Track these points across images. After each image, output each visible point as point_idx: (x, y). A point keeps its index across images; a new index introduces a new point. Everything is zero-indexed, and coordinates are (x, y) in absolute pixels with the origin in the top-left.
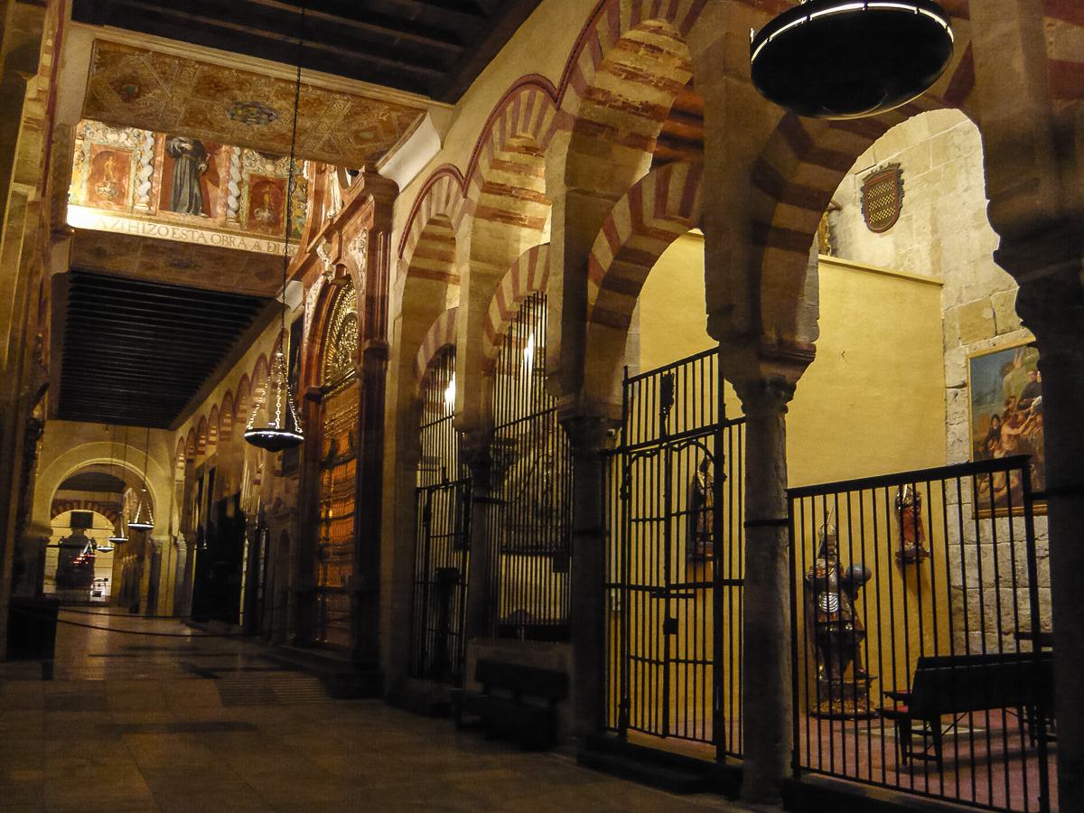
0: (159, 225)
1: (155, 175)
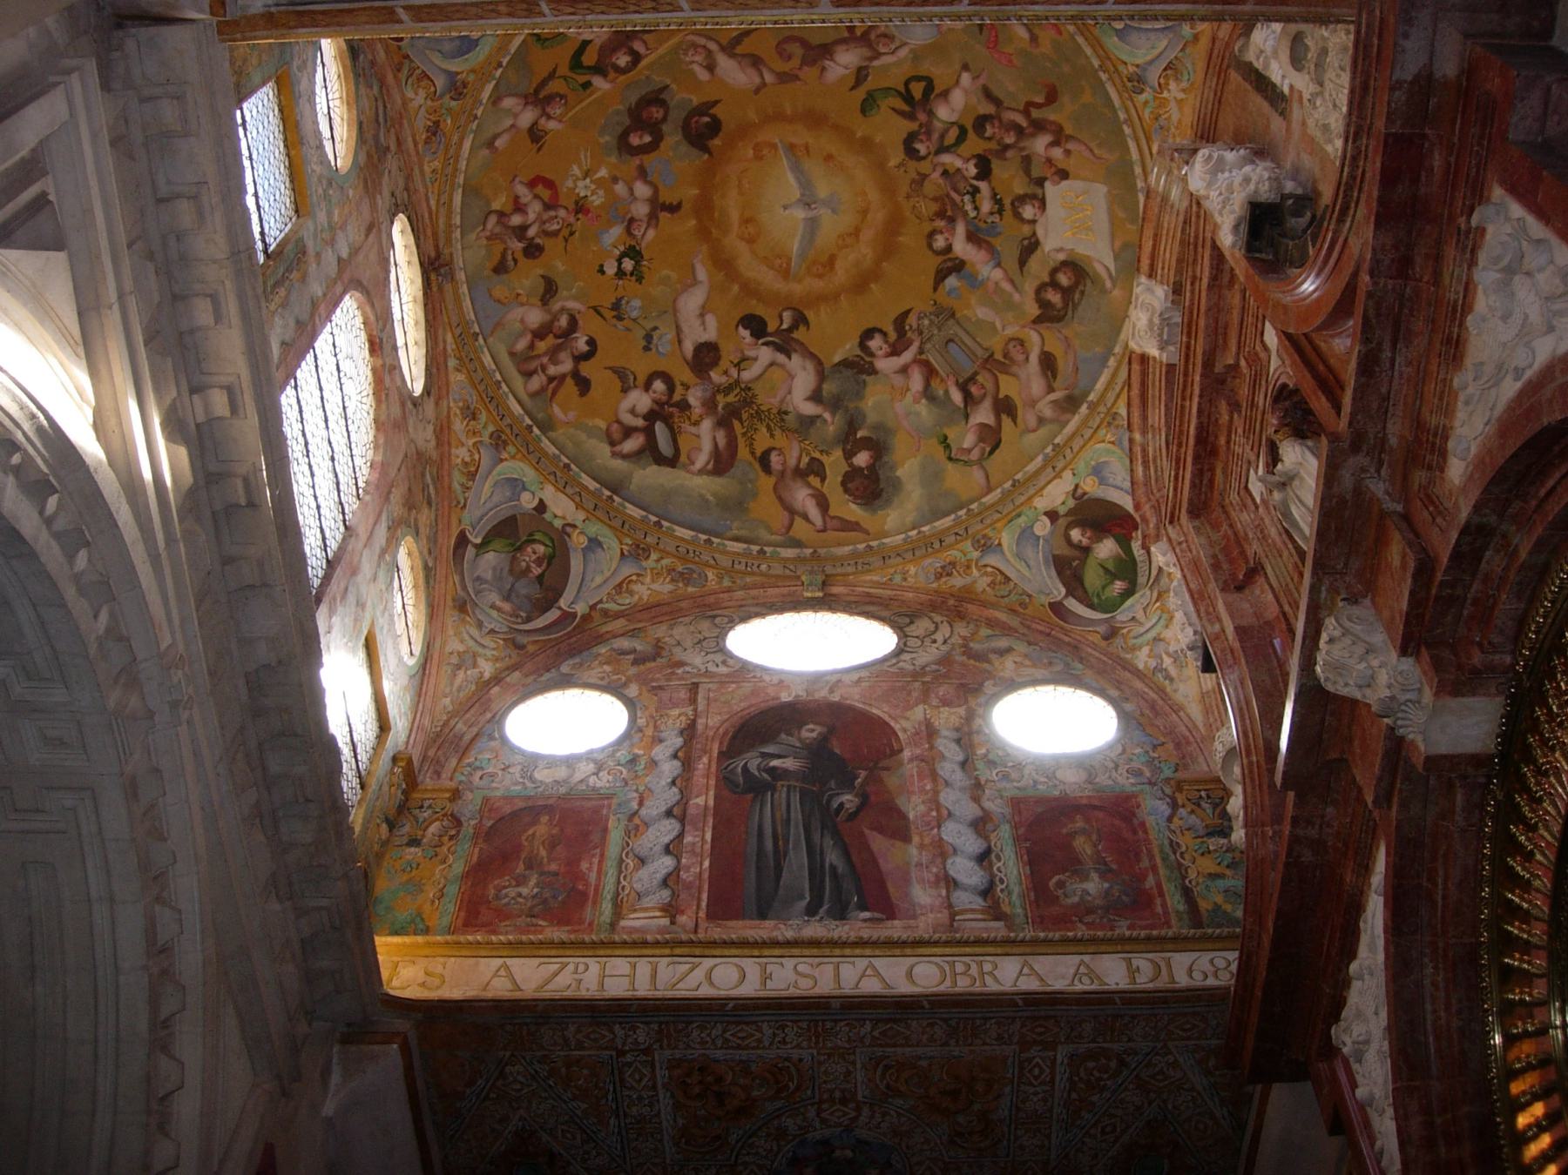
0: (708, 963)
1: (688, 839)
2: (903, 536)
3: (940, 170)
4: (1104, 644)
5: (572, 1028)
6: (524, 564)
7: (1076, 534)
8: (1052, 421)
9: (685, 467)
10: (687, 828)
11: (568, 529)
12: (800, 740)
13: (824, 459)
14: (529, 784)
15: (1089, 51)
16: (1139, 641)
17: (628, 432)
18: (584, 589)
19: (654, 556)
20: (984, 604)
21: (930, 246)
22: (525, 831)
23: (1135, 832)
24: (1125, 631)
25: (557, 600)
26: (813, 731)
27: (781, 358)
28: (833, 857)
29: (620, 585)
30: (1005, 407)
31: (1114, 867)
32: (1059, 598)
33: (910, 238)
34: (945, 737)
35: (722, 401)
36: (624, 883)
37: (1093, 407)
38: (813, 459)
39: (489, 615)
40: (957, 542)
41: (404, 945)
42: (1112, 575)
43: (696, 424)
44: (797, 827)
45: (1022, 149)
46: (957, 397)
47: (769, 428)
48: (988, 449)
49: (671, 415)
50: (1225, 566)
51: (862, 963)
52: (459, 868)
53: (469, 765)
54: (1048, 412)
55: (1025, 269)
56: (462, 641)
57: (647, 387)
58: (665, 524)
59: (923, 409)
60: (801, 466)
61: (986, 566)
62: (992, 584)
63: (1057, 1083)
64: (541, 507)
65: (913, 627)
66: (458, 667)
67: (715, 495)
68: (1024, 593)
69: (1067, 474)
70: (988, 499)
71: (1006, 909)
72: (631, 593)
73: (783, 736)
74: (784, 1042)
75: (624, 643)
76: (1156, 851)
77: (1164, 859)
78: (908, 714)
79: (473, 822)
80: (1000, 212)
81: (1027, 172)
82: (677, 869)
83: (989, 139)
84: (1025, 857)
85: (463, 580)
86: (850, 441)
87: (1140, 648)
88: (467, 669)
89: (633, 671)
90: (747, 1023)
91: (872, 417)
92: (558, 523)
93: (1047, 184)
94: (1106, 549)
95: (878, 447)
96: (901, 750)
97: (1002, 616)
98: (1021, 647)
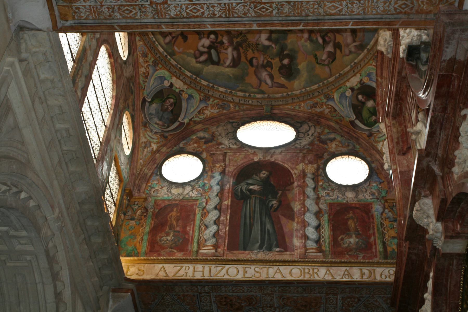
0: (227, 267)
1: (222, 218)
2: (300, 91)
4: (367, 138)
5: (185, 287)
6: (166, 107)
7: (360, 97)
8: (355, 53)
9: (222, 65)
10: (222, 214)
11: (181, 92)
12: (260, 178)
13: (273, 61)
14: (170, 195)
16: (380, 139)
17: (202, 53)
18: (187, 114)
19: (211, 100)
20: (327, 119)
22: (169, 214)
23: (369, 219)
24: (375, 135)
25: (178, 118)
26: (264, 174)
28: (268, 226)
29: (200, 111)
30: (337, 46)
31: (361, 233)
32: (353, 119)
34: (309, 177)
35: (235, 41)
36: (201, 236)
37: (368, 50)
38: (268, 61)
39: (155, 127)
40: (318, 96)
41: (131, 260)
43: (226, 49)
44: (257, 213)
46: (320, 41)
47: (252, 50)
48: (331, 61)
49: (217, 47)
50: (401, 143)
51: (276, 268)
52: (147, 229)
53: (150, 186)
54: (353, 49)
56: (146, 138)
57: (208, 37)
58: (215, 86)
59: (308, 44)
60: (264, 64)
61: (328, 105)
62: (330, 112)
63: (338, 305)
64: (172, 85)
65: (301, 128)
66: (145, 147)
68: (341, 116)
69: (358, 75)
70: (331, 80)
71: (323, 248)
72: (204, 114)
73: (254, 176)
74: (251, 291)
75: (201, 134)
76: (375, 227)
77: (378, 230)
78: (297, 167)
79: (152, 210)
82: (218, 230)
84: (332, 228)
85: (145, 116)
86: (281, 55)
88: (148, 148)
89: (204, 147)
90: (239, 286)
91: (289, 47)
92: (177, 90)
95: (292, 57)
96: (294, 183)
97: (333, 124)
98: (339, 138)
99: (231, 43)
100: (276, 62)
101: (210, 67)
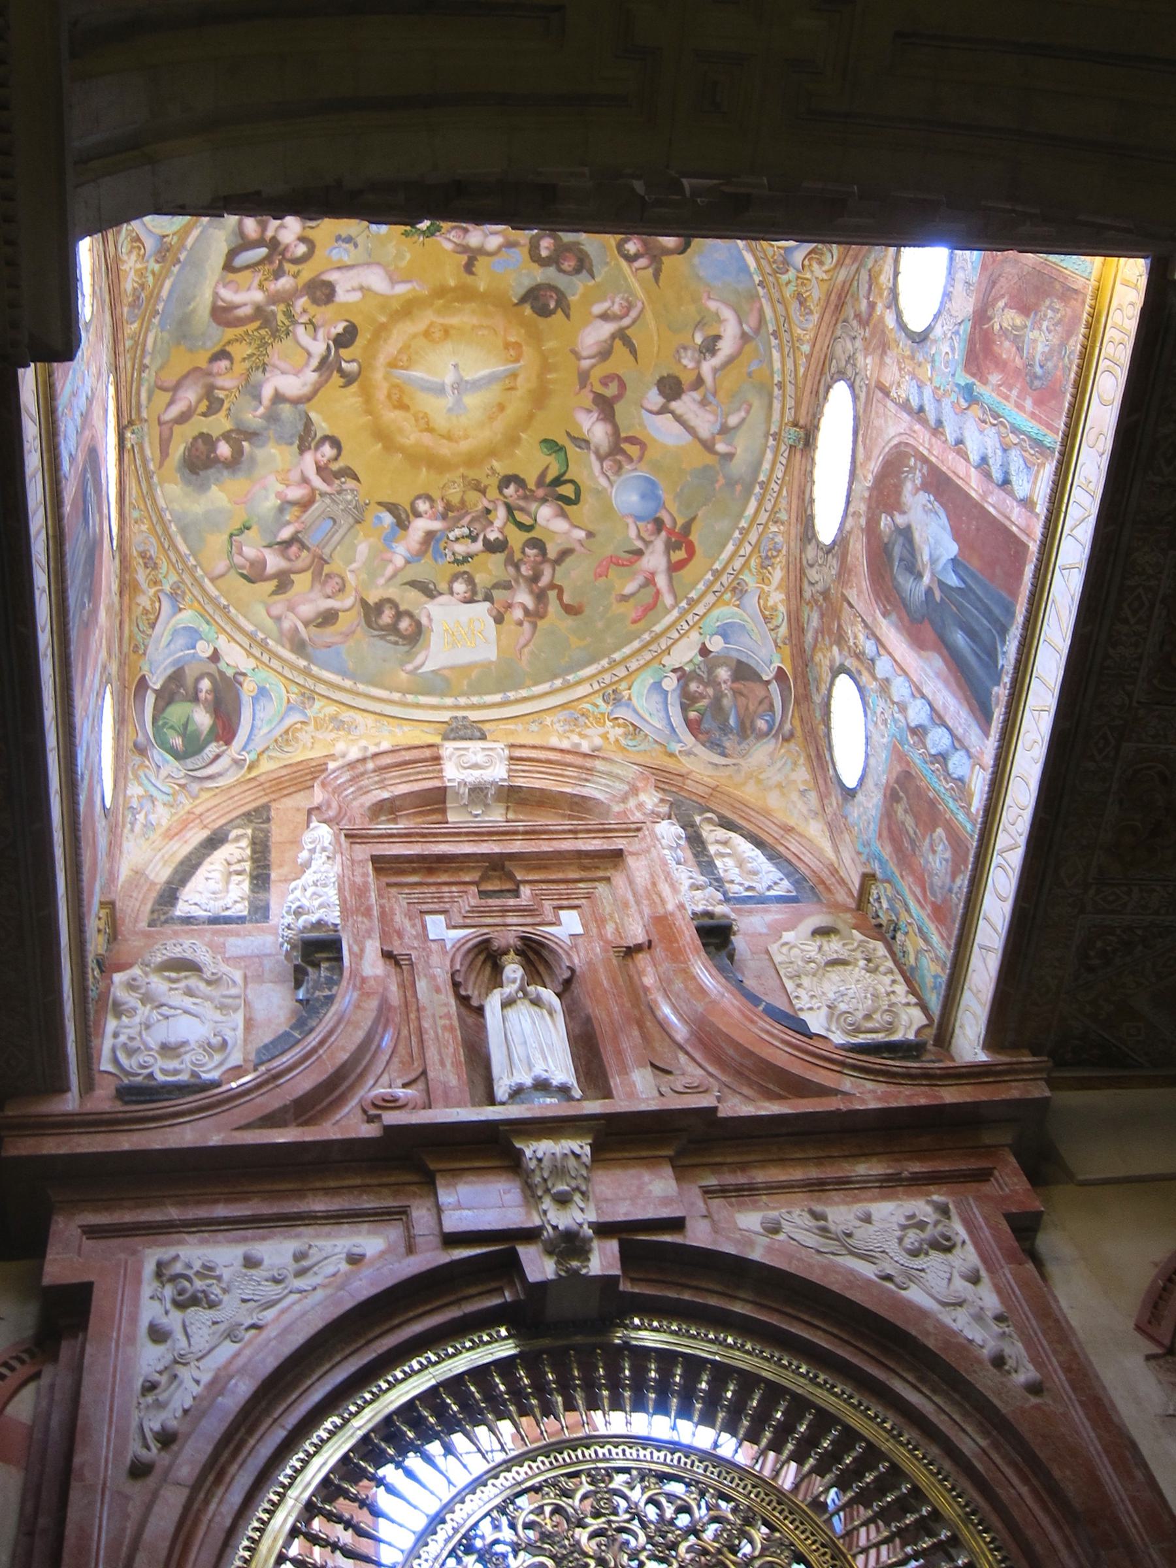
3: (490, 507)
7: (205, 684)
13: (223, 413)
15: (627, 650)
21: (419, 497)
27: (315, 363)
30: (283, 582)
33: (424, 478)
38: (222, 401)
42: (183, 735)
43: (261, 286)
45: (517, 582)
46: (286, 534)
48: (245, 572)
54: (286, 625)
55: (408, 587)
59: (272, 502)
67: (194, 311)
80: (456, 561)
81: (496, 586)
83: (523, 552)
87: (141, 784)
91: (261, 454)
93: (487, 605)
94: (203, 719)
95: (234, 463)
99: (274, 299)
100: (220, 424)
101: (223, 248)
